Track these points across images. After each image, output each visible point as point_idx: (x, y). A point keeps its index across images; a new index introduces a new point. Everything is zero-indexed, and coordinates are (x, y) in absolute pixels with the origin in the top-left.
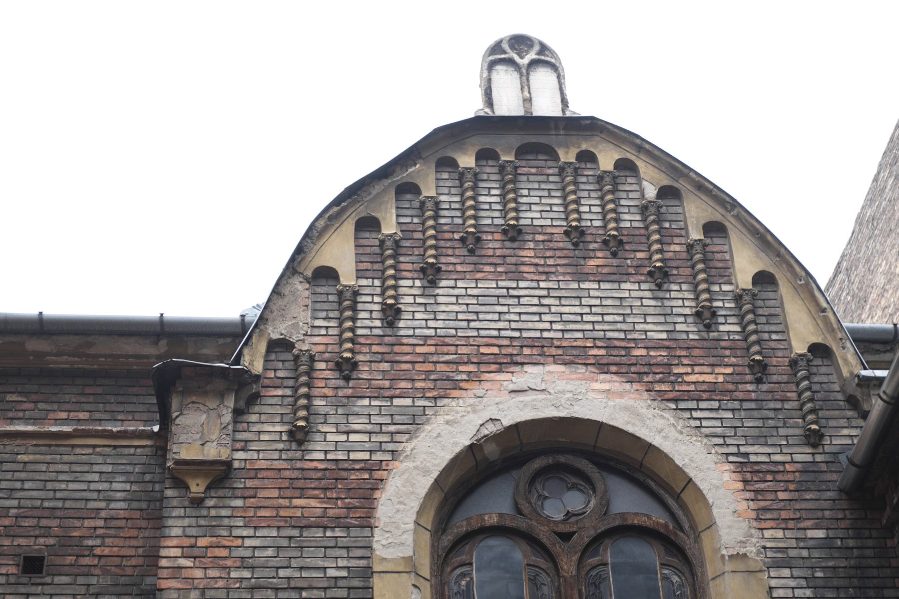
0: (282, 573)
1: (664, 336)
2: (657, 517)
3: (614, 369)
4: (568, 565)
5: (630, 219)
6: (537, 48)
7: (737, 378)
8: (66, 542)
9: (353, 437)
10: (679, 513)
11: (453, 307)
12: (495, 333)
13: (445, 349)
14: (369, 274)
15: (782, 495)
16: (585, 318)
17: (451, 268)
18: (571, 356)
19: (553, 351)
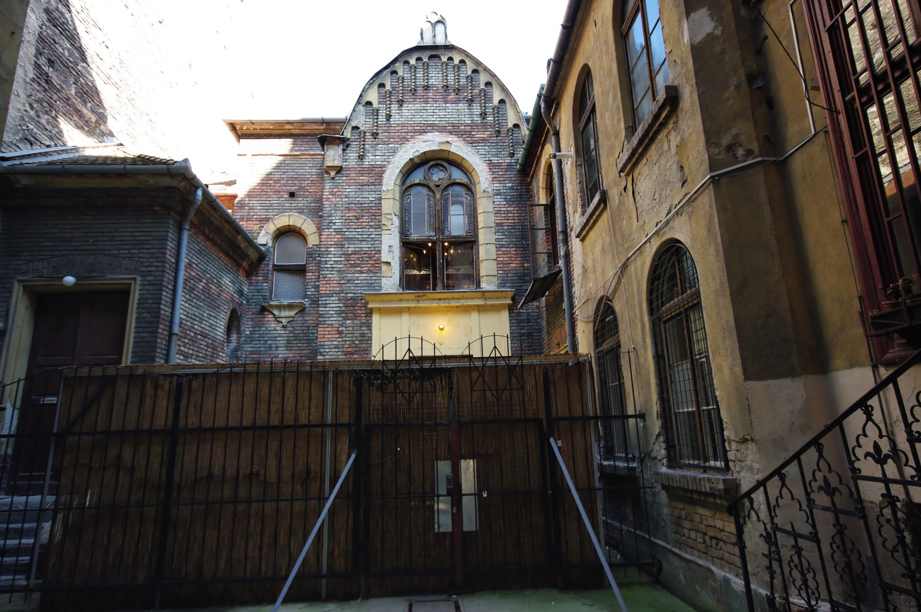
2: (465, 180)
4: (438, 196)
5: (463, 81)
11: (409, 113)
18: (442, 129)
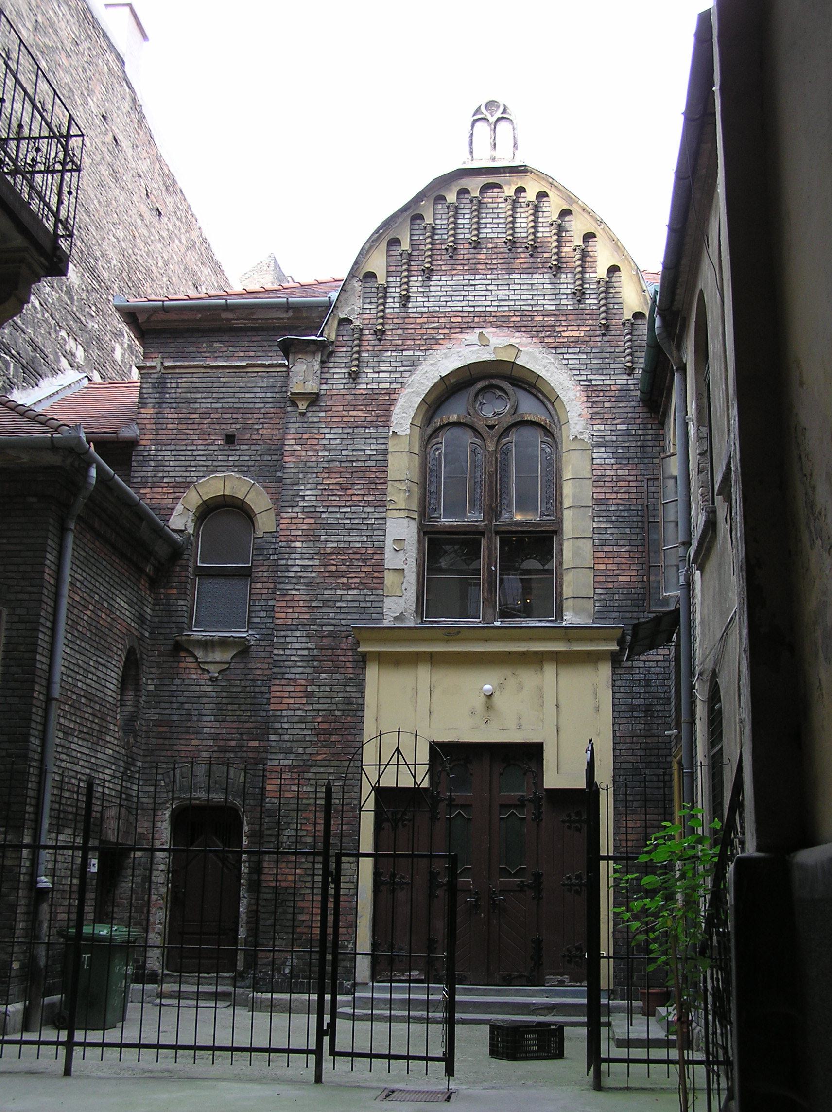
0: (344, 453)
1: (554, 308)
2: (541, 417)
3: (523, 329)
6: (501, 109)
7: (592, 333)
8: (246, 427)
9: (381, 375)
10: (553, 412)
12: (460, 309)
13: (432, 320)
14: (394, 274)
15: (606, 405)
16: (511, 297)
17: (439, 268)
18: (501, 322)
19: (491, 319)
